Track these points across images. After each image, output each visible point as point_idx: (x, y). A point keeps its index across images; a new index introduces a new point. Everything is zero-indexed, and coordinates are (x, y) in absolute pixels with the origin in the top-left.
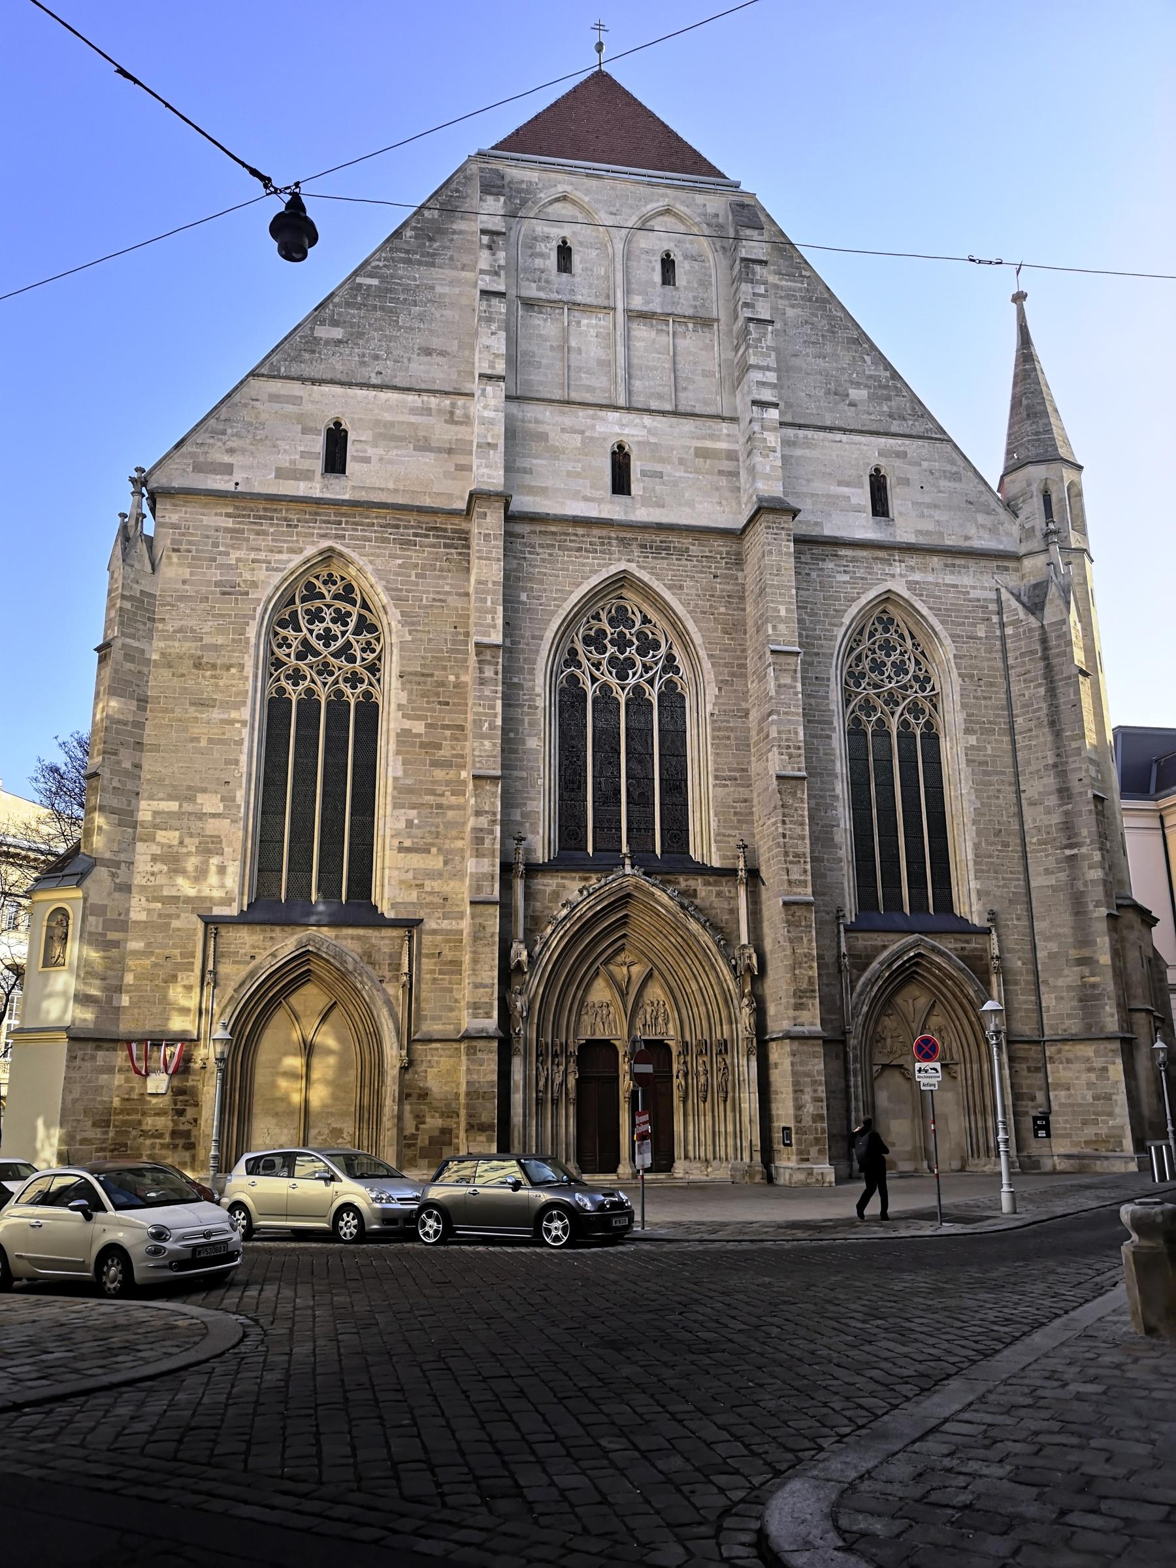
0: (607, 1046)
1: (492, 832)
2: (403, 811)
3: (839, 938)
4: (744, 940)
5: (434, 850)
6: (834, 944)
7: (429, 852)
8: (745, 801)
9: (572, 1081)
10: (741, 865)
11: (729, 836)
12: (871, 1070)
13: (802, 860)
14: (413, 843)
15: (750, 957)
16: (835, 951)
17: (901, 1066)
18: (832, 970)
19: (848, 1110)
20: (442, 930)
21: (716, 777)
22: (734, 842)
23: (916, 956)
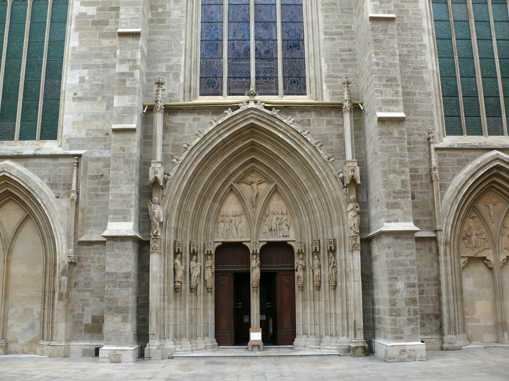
0: (240, 247)
1: (131, 75)
2: (77, 71)
3: (430, 155)
4: (349, 156)
5: (99, 98)
6: (426, 160)
7: (95, 99)
8: (350, 50)
9: (209, 274)
11: (337, 77)
12: (459, 262)
13: (394, 84)
14: (85, 94)
15: (353, 170)
16: (427, 166)
17: (484, 258)
18: (425, 181)
19: (439, 294)
20: (104, 158)
21: (326, 33)
22: (340, 82)
23: (494, 167)
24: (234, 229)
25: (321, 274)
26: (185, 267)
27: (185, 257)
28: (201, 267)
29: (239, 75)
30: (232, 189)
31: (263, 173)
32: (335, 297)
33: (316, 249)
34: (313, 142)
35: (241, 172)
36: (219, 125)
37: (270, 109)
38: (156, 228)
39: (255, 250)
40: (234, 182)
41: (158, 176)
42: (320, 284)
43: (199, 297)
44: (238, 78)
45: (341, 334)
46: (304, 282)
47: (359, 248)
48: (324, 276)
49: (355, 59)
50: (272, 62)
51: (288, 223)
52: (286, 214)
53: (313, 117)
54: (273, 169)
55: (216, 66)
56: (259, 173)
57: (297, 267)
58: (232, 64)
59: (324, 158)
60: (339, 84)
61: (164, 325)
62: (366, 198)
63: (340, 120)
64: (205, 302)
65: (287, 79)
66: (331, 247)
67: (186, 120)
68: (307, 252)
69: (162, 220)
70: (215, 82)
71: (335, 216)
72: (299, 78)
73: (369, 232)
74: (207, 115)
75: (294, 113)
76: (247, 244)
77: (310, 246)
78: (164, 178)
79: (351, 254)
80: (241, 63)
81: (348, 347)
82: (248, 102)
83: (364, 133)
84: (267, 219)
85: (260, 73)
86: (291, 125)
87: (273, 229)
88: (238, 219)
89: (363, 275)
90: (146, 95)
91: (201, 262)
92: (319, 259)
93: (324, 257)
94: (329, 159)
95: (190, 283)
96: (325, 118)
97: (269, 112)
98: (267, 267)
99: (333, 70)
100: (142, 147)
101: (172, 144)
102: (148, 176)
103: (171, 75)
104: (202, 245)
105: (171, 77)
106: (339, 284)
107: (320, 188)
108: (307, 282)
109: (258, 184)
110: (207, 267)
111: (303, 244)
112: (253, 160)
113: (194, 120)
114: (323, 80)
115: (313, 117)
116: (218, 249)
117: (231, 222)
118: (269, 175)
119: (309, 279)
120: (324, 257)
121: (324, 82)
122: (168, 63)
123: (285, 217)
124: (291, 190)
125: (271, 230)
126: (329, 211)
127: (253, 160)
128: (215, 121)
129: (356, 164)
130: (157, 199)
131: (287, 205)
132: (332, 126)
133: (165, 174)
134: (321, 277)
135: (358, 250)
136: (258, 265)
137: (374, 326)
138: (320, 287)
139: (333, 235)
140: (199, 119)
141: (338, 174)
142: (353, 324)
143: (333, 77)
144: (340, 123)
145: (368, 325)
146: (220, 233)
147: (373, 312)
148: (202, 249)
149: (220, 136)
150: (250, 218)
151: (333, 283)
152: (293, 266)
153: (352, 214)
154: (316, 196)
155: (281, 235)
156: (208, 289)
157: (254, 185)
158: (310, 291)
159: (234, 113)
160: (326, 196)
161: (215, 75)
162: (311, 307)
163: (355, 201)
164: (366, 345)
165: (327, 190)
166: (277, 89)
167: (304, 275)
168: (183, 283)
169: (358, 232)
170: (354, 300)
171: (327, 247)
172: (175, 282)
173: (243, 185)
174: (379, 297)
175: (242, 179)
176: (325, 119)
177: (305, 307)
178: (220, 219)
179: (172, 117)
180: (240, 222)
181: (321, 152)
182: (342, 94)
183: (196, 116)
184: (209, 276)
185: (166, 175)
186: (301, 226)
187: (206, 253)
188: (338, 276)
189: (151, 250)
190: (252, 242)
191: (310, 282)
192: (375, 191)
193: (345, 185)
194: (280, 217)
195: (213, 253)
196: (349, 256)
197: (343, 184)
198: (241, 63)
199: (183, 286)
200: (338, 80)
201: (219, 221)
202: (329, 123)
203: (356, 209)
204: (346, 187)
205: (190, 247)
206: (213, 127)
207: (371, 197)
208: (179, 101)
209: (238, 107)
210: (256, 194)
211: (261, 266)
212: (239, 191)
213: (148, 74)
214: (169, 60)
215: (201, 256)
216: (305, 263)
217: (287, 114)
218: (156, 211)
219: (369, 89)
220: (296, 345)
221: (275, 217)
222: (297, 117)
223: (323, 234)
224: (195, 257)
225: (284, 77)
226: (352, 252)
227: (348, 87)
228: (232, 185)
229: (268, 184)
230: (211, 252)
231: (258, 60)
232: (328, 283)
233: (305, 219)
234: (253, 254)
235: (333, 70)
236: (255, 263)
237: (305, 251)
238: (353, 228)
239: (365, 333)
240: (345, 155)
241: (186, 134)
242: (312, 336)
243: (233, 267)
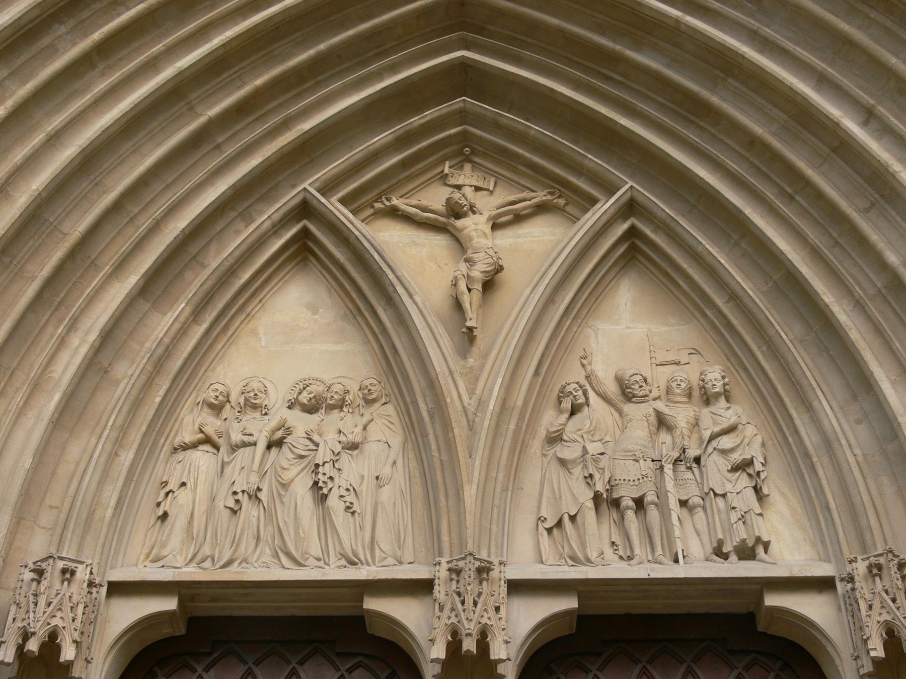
39: (470, 627)
87: (626, 493)
112: (462, 116)
117: (275, 444)
146: (178, 522)
180: (354, 446)
221: (638, 412)
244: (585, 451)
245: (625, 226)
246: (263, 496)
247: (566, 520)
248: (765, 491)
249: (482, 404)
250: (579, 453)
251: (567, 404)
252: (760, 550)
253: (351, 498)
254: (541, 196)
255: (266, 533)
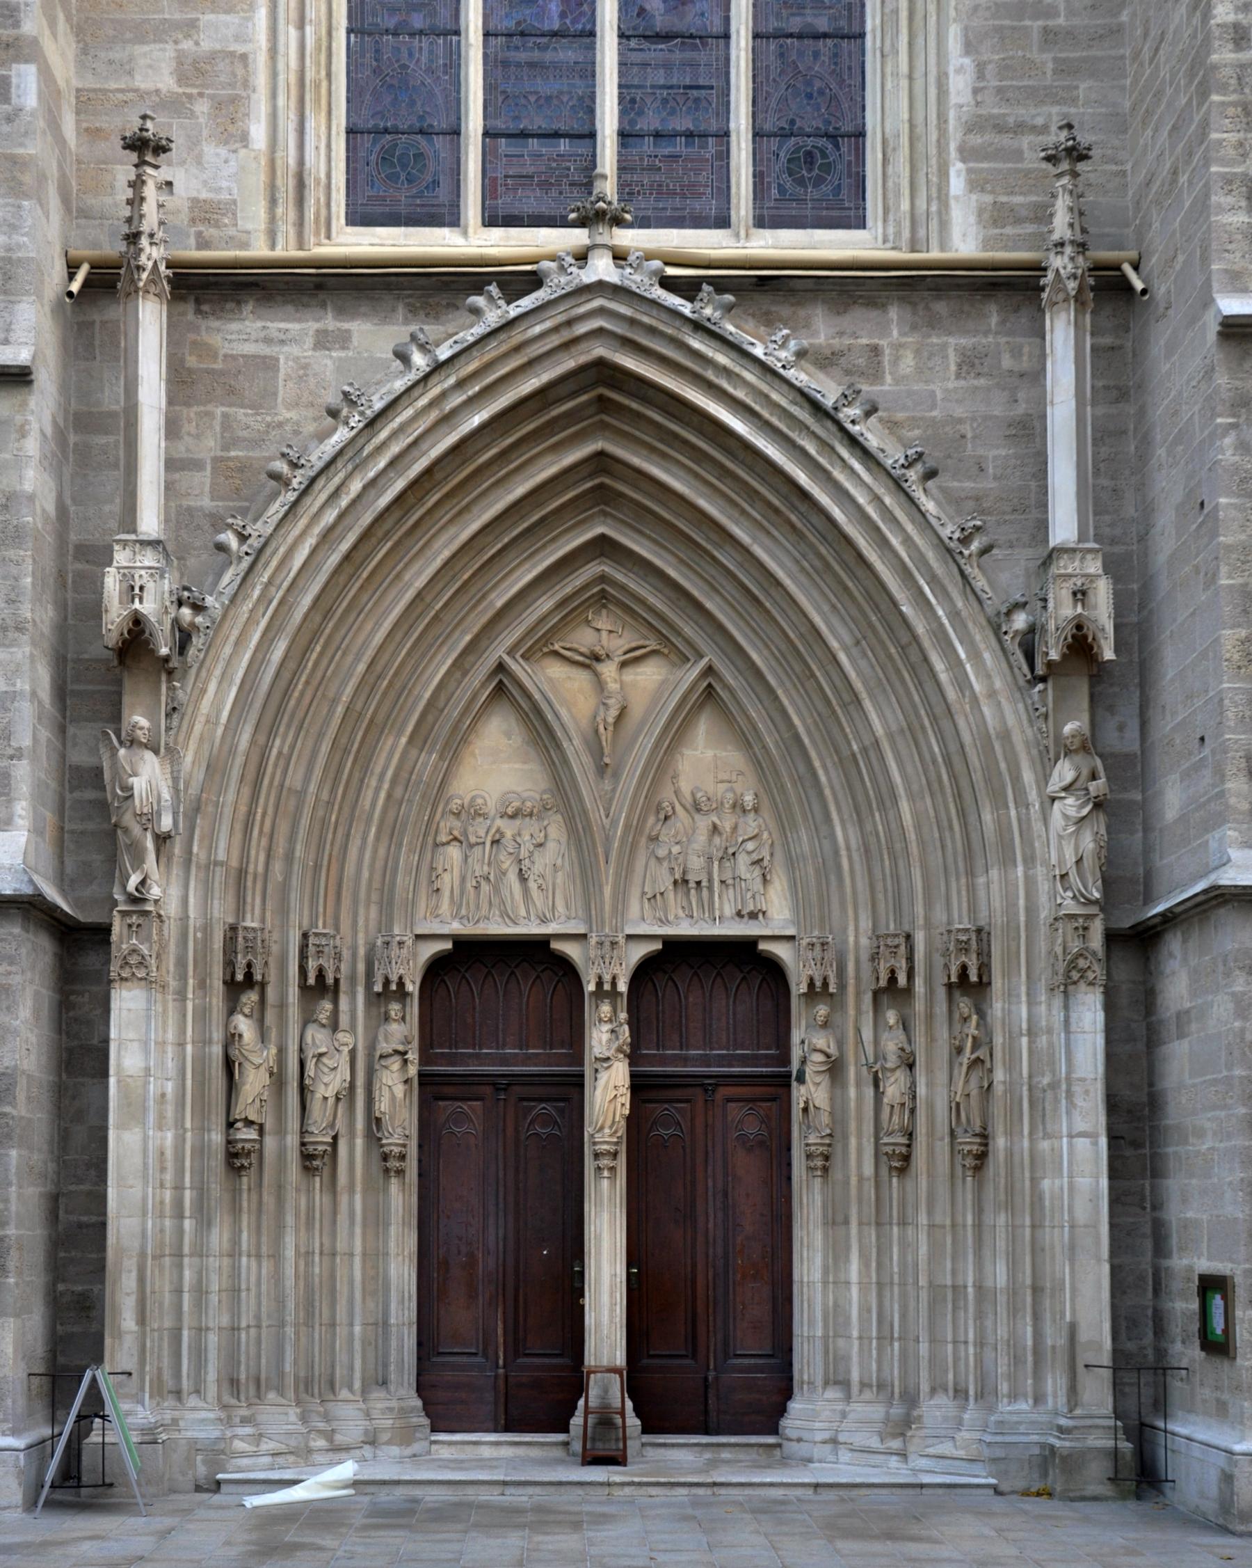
10: (1061, 225)
11: (1020, 128)
15: (1080, 595)
22: (1030, 149)
24: (512, 877)
25: (914, 1097)
26: (282, 1051)
27: (282, 1006)
28: (353, 1053)
29: (537, 122)
30: (500, 687)
31: (651, 609)
32: (979, 1211)
33: (893, 979)
34: (893, 456)
35: (545, 604)
36: (439, 367)
37: (686, 289)
38: (139, 860)
39: (607, 978)
40: (511, 652)
41: (148, 607)
42: (909, 1146)
43: (344, 1200)
44: (533, 136)
45: (1004, 1387)
46: (836, 1136)
47: (1098, 971)
48: (931, 1106)
49: (1116, 32)
50: (702, 56)
51: (765, 853)
52: (756, 810)
53: (895, 333)
54: (696, 593)
55: (430, 71)
56: (631, 609)
57: (804, 1062)
58: (505, 64)
59: (945, 533)
60: (1026, 165)
61: (180, 1329)
62: (1137, 734)
63: (1026, 350)
64: (376, 1221)
65: (774, 143)
66: (964, 968)
67: (282, 342)
68: (851, 990)
69: (166, 823)
70: (419, 156)
71: (987, 817)
72: (833, 137)
73: (1148, 899)
74: (385, 320)
75: (802, 313)
76: (571, 950)
77: (866, 967)
78: (176, 622)
79: (1058, 1001)
80: (548, 56)
81: (1037, 1451)
82: (582, 257)
83: (1142, 413)
84: (667, 834)
85: (640, 113)
86: (790, 374)
87: (692, 878)
88: (529, 830)
89: (1113, 1105)
90: (75, 211)
91: (353, 1029)
92: (905, 1026)
93: (930, 1017)
94: (965, 541)
95: (303, 1132)
96: (952, 340)
97: (686, 308)
98: (663, 1060)
99: (1000, 91)
100: (67, 471)
101: (215, 460)
102: (95, 610)
103: (202, 107)
104: (362, 952)
105: (201, 120)
106: (1000, 1143)
107: (920, 684)
108: (846, 1138)
109: (624, 665)
110: (381, 1057)
111: (830, 955)
113: (323, 341)
114: (953, 147)
115: (895, 333)
116: (437, 970)
117: (495, 842)
118: (679, 622)
119: (860, 1120)
120: (930, 1017)
121: (953, 153)
122: (187, 45)
123: (751, 825)
124: (780, 692)
125: (681, 883)
126: (959, 796)
127: (603, 547)
128: (423, 348)
129: (1099, 564)
130: (143, 722)
131: (761, 765)
132: (982, 382)
133: (180, 603)
134: (913, 1111)
135: (1091, 984)
136: (620, 1050)
137: (1161, 1353)
138: (906, 1158)
139: (973, 909)
140: (343, 340)
141: (1009, 613)
142: (1062, 1342)
143: (1000, 128)
144: (1025, 364)
145: (1130, 1346)
147: (1157, 1291)
148: (361, 967)
149: (448, 419)
150: (588, 827)
151: (969, 1143)
152: (785, 1059)
153: (1070, 806)
154: (896, 719)
155: (729, 911)
156: (385, 1157)
157: (608, 670)
158: (861, 1179)
159: (513, 311)
160: (946, 724)
161: (421, 118)
162: (864, 1257)
163: (1084, 748)
164: (1126, 1446)
165: (951, 694)
166: (724, 191)
167: (832, 1099)
168: (268, 1127)
169: (1097, 895)
170: (1072, 1227)
171: (946, 966)
172: (230, 1125)
173: (556, 670)
174: (1190, 1214)
175: (547, 638)
176: (954, 343)
177: (836, 1254)
178: (448, 825)
179: (215, 324)
180: (541, 845)
181: (929, 506)
182: (1043, 215)
183: (330, 322)
184: (393, 1097)
185: (186, 612)
186: (829, 867)
187: (378, 988)
188: (998, 1109)
189: (114, 968)
190: (593, 940)
191: (859, 1137)
192: (1190, 697)
193: (1040, 670)
194: (727, 825)
195: (412, 987)
196: (1049, 1011)
197: (1032, 667)
198: (548, 56)
199: (270, 1142)
200: (1026, 141)
201: (443, 838)
202: (970, 363)
203: (1093, 786)
204: (1043, 679)
205: (303, 957)
206: (413, 376)
207: (1165, 726)
208: (245, 245)
209: (534, 281)
210: (613, 713)
211: (634, 1058)
212: (537, 696)
213: (86, 101)
214: (192, 25)
215: (353, 1004)
216: (840, 1044)
217: (769, 321)
218: (139, 784)
219: (1183, 179)
220: (790, 1433)
221: (703, 823)
222: (815, 334)
223: (928, 905)
224: (327, 1005)
225: (757, 134)
226: (1065, 992)
227: (1075, 174)
228: (501, 667)
229: (674, 665)
230: (401, 984)
231: (633, 43)
232: (947, 1140)
233: (844, 833)
234: (600, 993)
235: (1000, 91)
236: (605, 1037)
237: (842, 986)
238: (1073, 877)
239: (1117, 1386)
240: (1043, 526)
241: (286, 414)
242: (868, 1395)
243: (504, 1060)
244: (670, 852)
245: (705, 684)
246: (492, 877)
247: (658, 896)
248: (768, 877)
249: (614, 823)
250: (666, 852)
251: (662, 816)
252: (760, 916)
253: (540, 881)
254: (653, 644)
255: (495, 901)
